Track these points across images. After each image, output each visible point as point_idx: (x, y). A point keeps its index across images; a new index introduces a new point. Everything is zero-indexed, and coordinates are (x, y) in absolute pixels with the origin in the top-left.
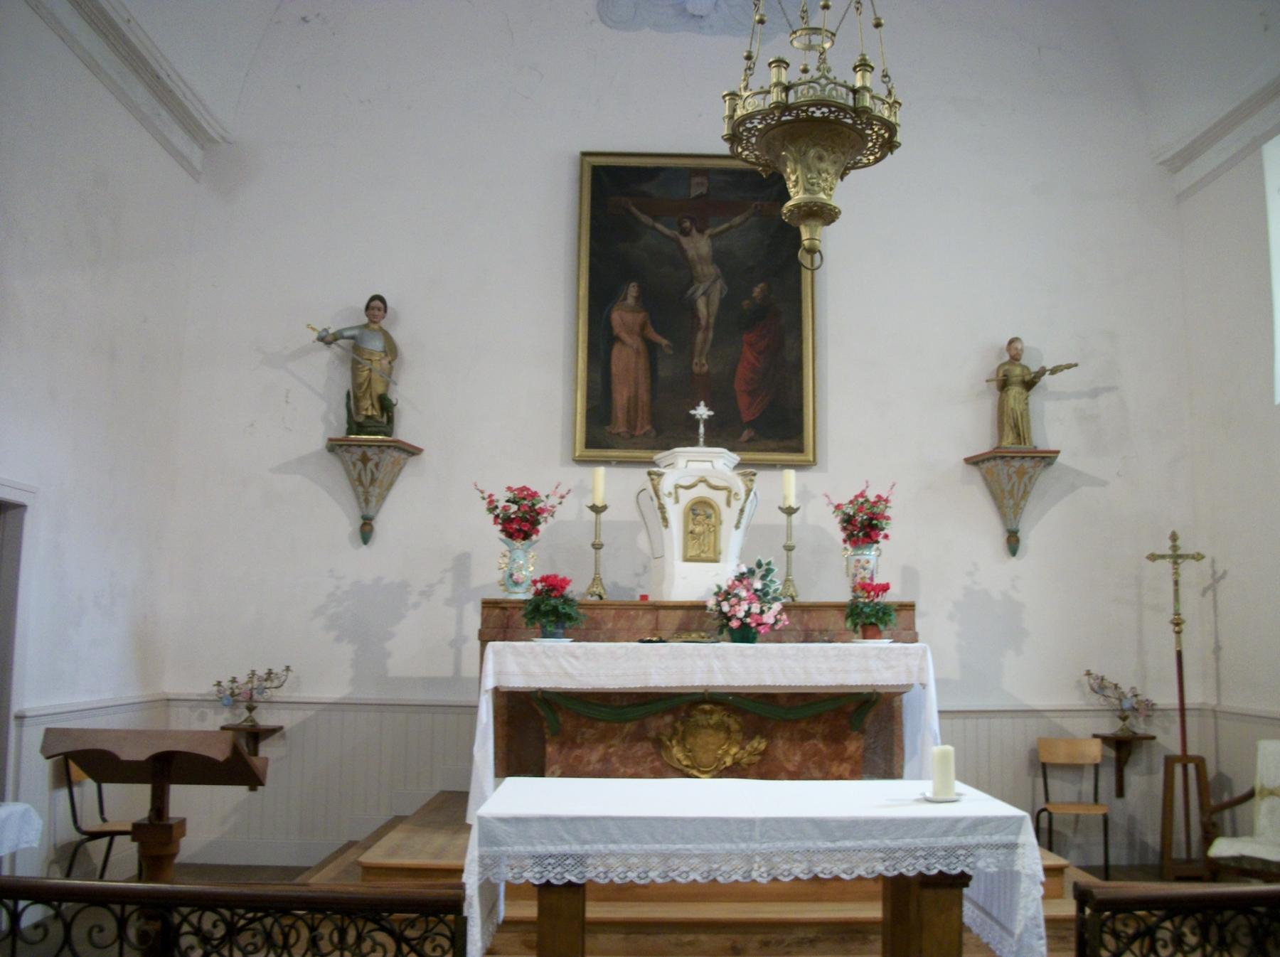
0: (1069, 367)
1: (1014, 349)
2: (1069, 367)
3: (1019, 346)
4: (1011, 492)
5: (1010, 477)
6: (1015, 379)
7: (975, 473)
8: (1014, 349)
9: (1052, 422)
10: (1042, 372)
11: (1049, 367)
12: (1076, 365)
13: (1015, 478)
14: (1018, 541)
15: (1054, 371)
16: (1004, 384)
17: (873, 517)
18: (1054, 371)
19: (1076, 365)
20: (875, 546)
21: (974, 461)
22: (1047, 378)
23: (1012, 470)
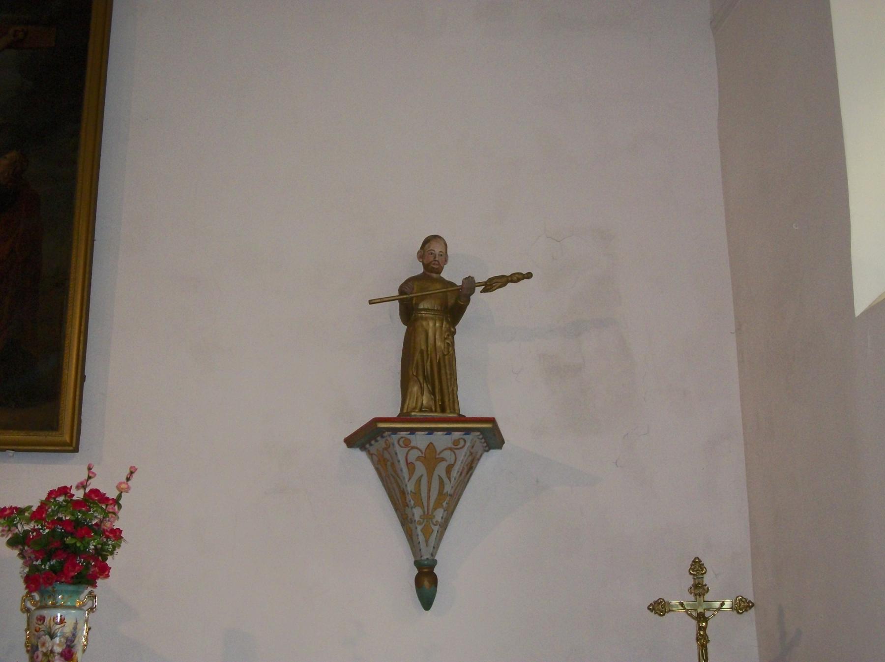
0: (517, 278)
1: (432, 253)
2: (517, 278)
3: (437, 248)
4: (417, 494)
5: (411, 466)
6: (432, 302)
7: (360, 457)
8: (432, 253)
9: (491, 368)
10: (470, 285)
11: (480, 278)
12: (529, 276)
13: (421, 469)
14: (434, 580)
15: (490, 285)
16: (409, 312)
17: (79, 529)
18: (490, 285)
19: (529, 276)
20: (90, 589)
21: (364, 438)
22: (478, 298)
23: (414, 455)
